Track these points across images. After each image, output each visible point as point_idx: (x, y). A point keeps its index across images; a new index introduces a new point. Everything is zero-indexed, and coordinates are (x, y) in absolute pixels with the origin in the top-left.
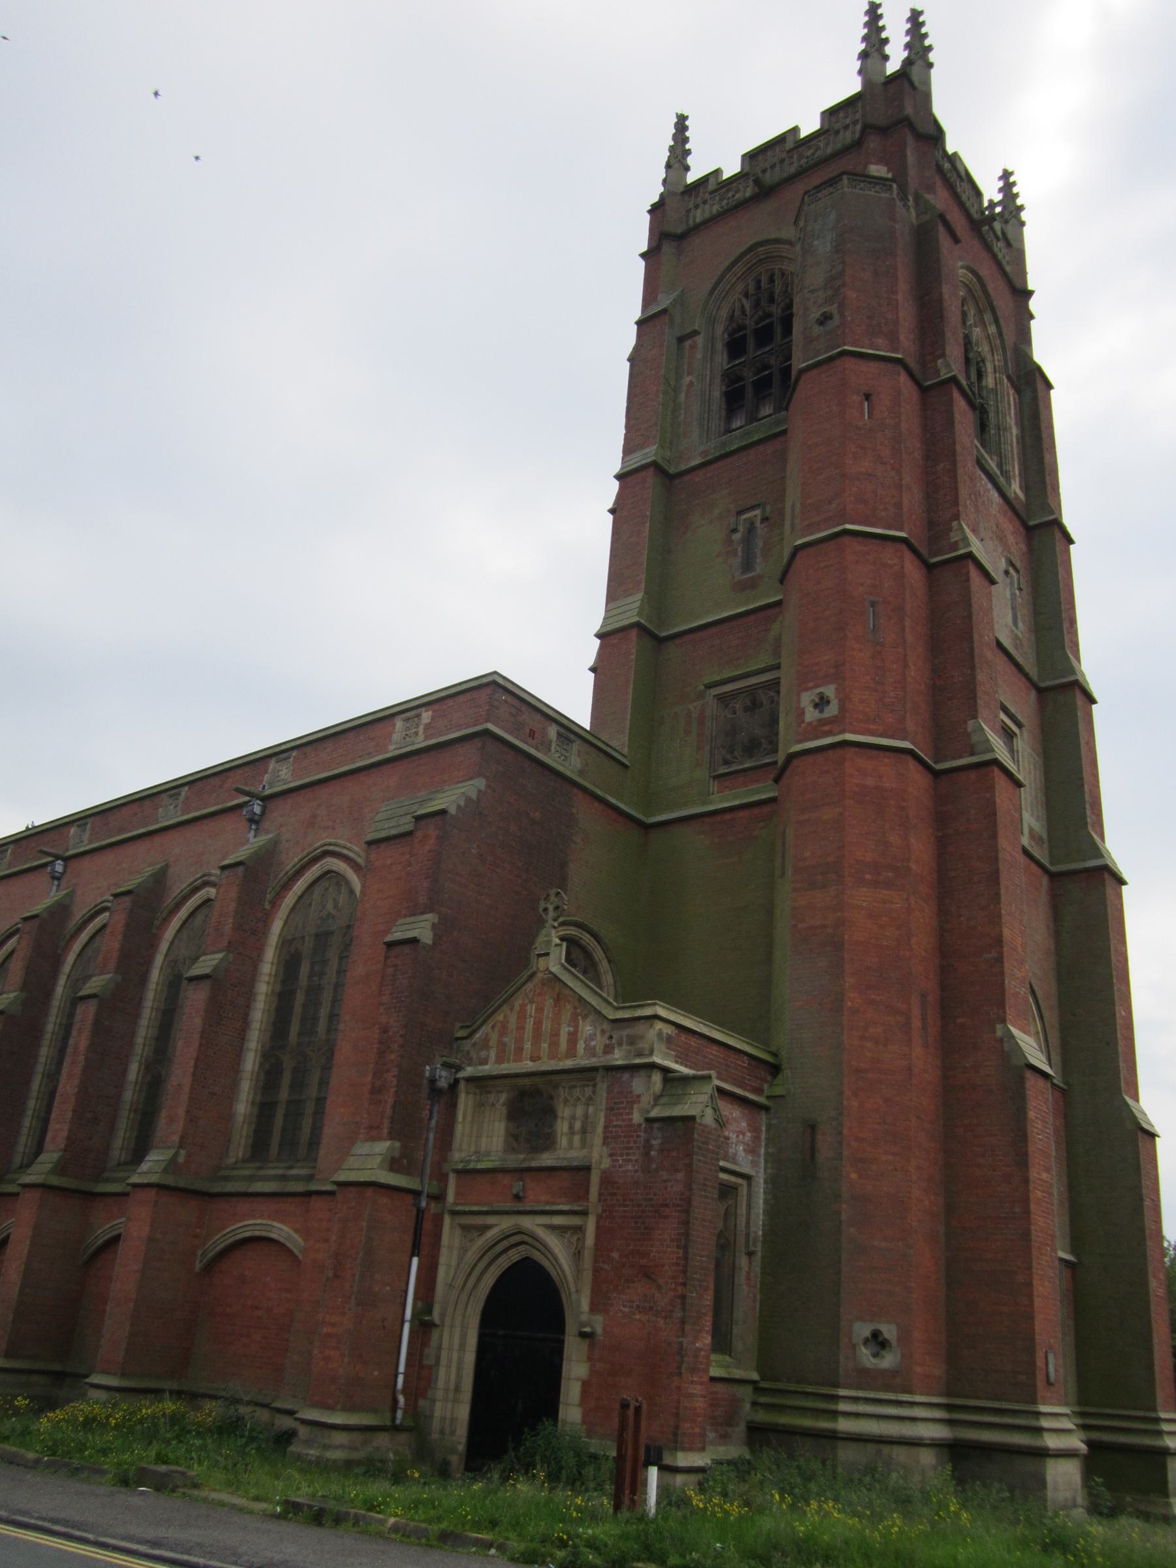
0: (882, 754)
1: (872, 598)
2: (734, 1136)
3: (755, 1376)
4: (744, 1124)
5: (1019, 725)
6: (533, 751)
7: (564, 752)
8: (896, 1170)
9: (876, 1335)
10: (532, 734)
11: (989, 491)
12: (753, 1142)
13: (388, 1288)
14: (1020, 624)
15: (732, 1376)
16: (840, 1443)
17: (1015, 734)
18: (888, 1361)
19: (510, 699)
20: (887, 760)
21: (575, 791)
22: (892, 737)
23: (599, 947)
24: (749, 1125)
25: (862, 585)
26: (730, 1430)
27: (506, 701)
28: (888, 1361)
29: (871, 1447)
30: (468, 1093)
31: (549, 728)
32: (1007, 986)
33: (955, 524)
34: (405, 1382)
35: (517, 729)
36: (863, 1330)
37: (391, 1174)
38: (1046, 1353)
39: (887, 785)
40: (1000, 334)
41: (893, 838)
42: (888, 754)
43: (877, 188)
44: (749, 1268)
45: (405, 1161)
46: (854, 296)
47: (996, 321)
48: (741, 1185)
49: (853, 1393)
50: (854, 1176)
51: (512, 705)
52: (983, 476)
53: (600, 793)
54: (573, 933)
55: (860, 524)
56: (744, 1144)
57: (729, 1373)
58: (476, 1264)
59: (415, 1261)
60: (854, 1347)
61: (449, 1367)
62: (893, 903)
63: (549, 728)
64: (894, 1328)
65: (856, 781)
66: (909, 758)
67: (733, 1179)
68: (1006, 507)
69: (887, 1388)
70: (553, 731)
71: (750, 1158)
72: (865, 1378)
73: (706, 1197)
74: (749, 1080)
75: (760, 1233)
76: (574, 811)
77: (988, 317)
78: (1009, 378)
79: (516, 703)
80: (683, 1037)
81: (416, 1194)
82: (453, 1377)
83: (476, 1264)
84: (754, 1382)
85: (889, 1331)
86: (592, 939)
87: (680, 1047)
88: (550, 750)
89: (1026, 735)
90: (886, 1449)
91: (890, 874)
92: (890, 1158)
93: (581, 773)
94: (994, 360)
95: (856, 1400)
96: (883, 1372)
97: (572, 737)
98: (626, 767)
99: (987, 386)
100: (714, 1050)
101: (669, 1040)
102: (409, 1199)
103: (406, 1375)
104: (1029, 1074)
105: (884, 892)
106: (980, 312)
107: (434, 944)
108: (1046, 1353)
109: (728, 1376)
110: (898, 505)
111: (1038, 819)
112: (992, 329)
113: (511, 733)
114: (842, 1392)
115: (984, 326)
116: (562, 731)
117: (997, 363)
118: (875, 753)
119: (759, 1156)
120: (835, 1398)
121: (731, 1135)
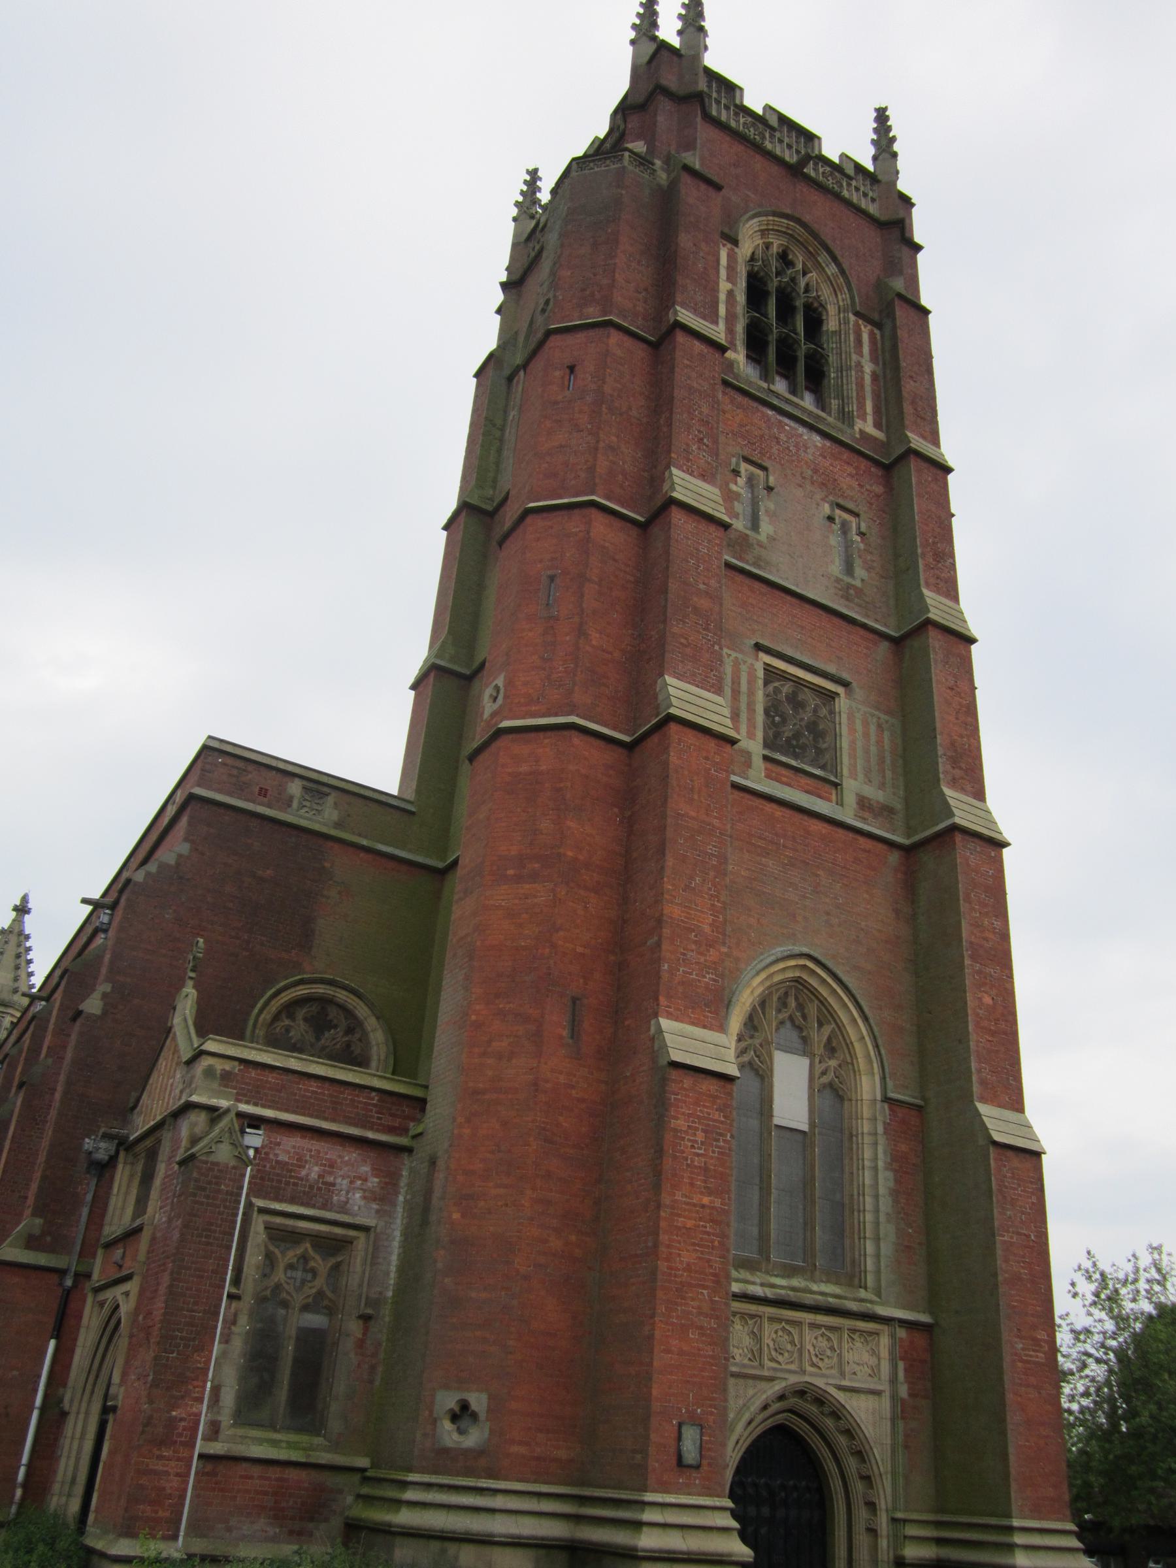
0: (541, 735)
1: (549, 573)
2: (345, 1182)
3: (362, 1462)
4: (365, 1169)
5: (845, 684)
6: (261, 809)
7: (315, 807)
8: (507, 1205)
9: (464, 1406)
10: (263, 792)
11: (801, 435)
12: (382, 1188)
13: (15, 1373)
14: (860, 572)
15: (312, 1460)
16: (398, 1541)
17: (838, 694)
18: (473, 1438)
19: (229, 761)
20: (546, 741)
21: (330, 844)
22: (556, 715)
23: (361, 1003)
24: (373, 1169)
25: (541, 561)
26: (311, 1525)
27: (224, 764)
28: (473, 1438)
29: (435, 1546)
30: (125, 1163)
31: (290, 784)
32: (665, 976)
33: (667, 474)
34: (28, 1475)
35: (240, 789)
36: (448, 1400)
37: (26, 1251)
38: (680, 1425)
39: (544, 767)
40: (842, 272)
41: (545, 825)
42: (549, 734)
43: (608, 162)
44: (364, 1334)
45: (49, 1239)
46: (569, 274)
47: (834, 259)
48: (357, 1238)
49: (426, 1478)
50: (456, 1216)
51: (233, 767)
52: (786, 420)
53: (365, 842)
54: (321, 991)
55: (545, 499)
56: (365, 1191)
57: (308, 1456)
58: (99, 1343)
59: (52, 1343)
60: (434, 1422)
61: (68, 1457)
62: (535, 897)
63: (290, 784)
64: (484, 1397)
65: (510, 770)
66: (574, 733)
67: (338, 1231)
68: (837, 449)
69: (469, 1472)
70: (295, 788)
71: (375, 1206)
72: (445, 1460)
73: (208, 1244)
74: (379, 1118)
75: (390, 1294)
76: (327, 865)
77: (823, 257)
78: (857, 314)
79: (241, 764)
80: (253, 1073)
81: (62, 1273)
82: (71, 1468)
83: (99, 1343)
84: (364, 1470)
85: (478, 1401)
86: (352, 996)
87: (246, 1084)
88: (290, 806)
89: (859, 693)
90: (452, 1548)
91: (536, 865)
92: (502, 1191)
93: (338, 825)
94: (838, 301)
95: (429, 1486)
96: (466, 1452)
97: (326, 789)
98: (413, 813)
99: (828, 330)
100: (313, 1086)
101: (226, 1077)
102: (55, 1278)
103: (29, 1466)
104: (674, 1074)
105: (527, 886)
106: (812, 256)
107: (105, 1013)
108: (680, 1425)
109: (304, 1460)
110: (591, 470)
111: (882, 786)
112: (832, 269)
113: (230, 794)
114: (413, 1477)
115: (818, 266)
116: (305, 783)
117: (841, 303)
118: (533, 735)
119: (394, 1204)
120: (404, 1485)
121: (339, 1180)
